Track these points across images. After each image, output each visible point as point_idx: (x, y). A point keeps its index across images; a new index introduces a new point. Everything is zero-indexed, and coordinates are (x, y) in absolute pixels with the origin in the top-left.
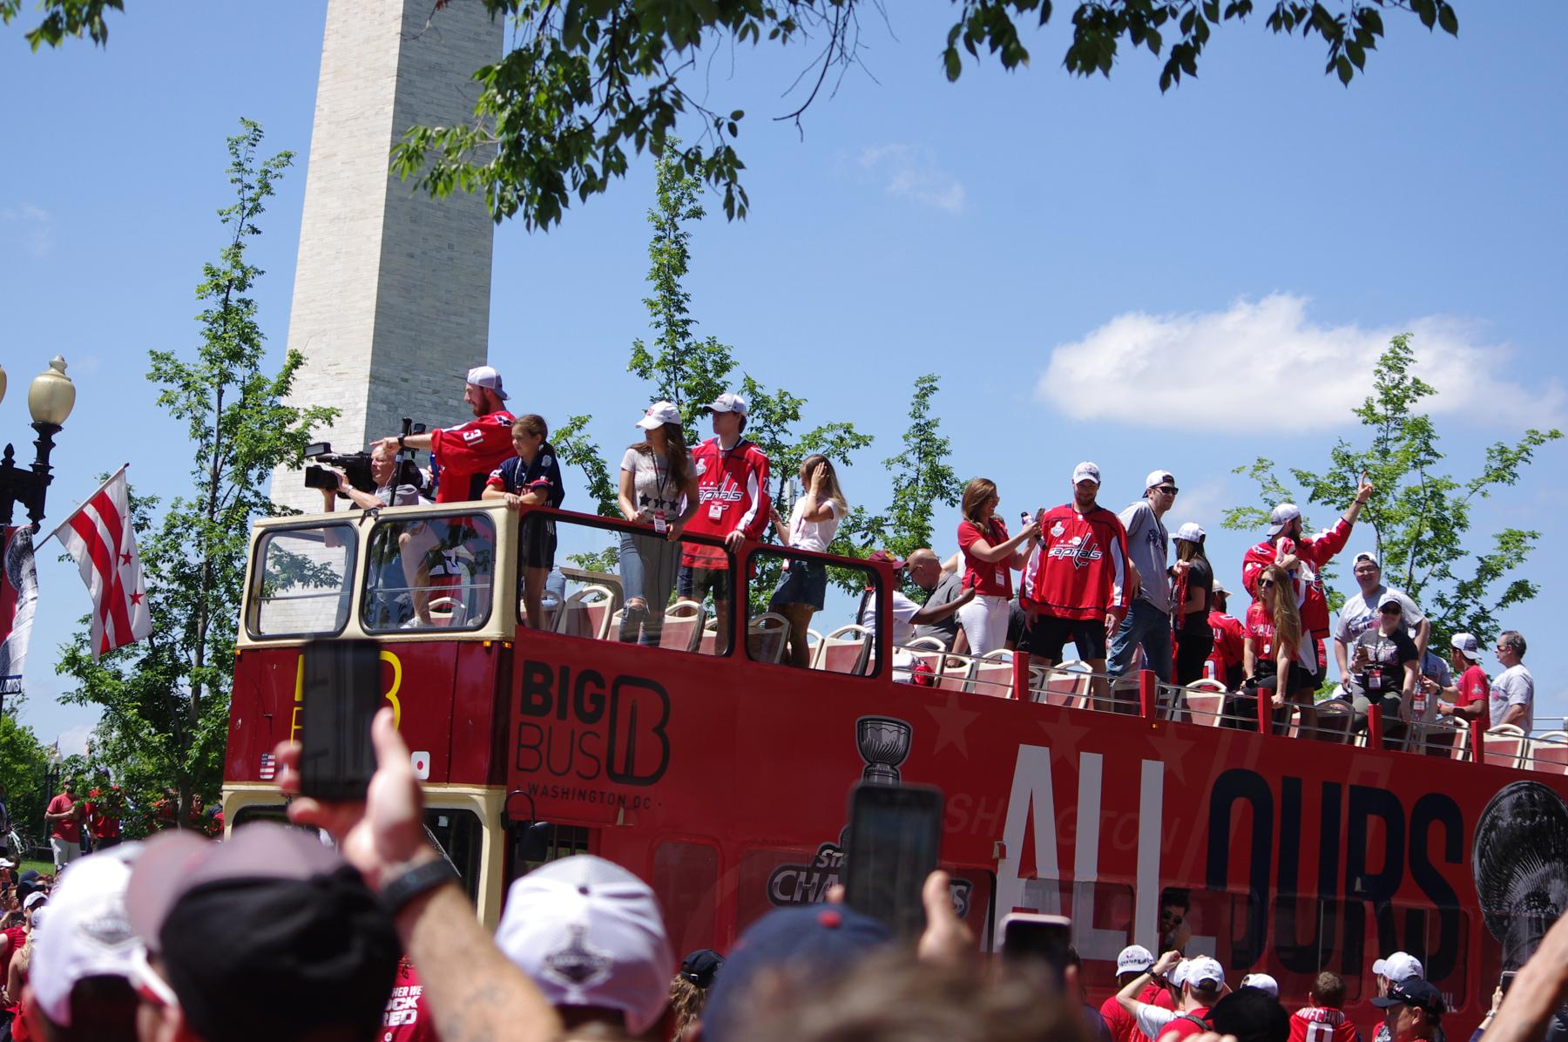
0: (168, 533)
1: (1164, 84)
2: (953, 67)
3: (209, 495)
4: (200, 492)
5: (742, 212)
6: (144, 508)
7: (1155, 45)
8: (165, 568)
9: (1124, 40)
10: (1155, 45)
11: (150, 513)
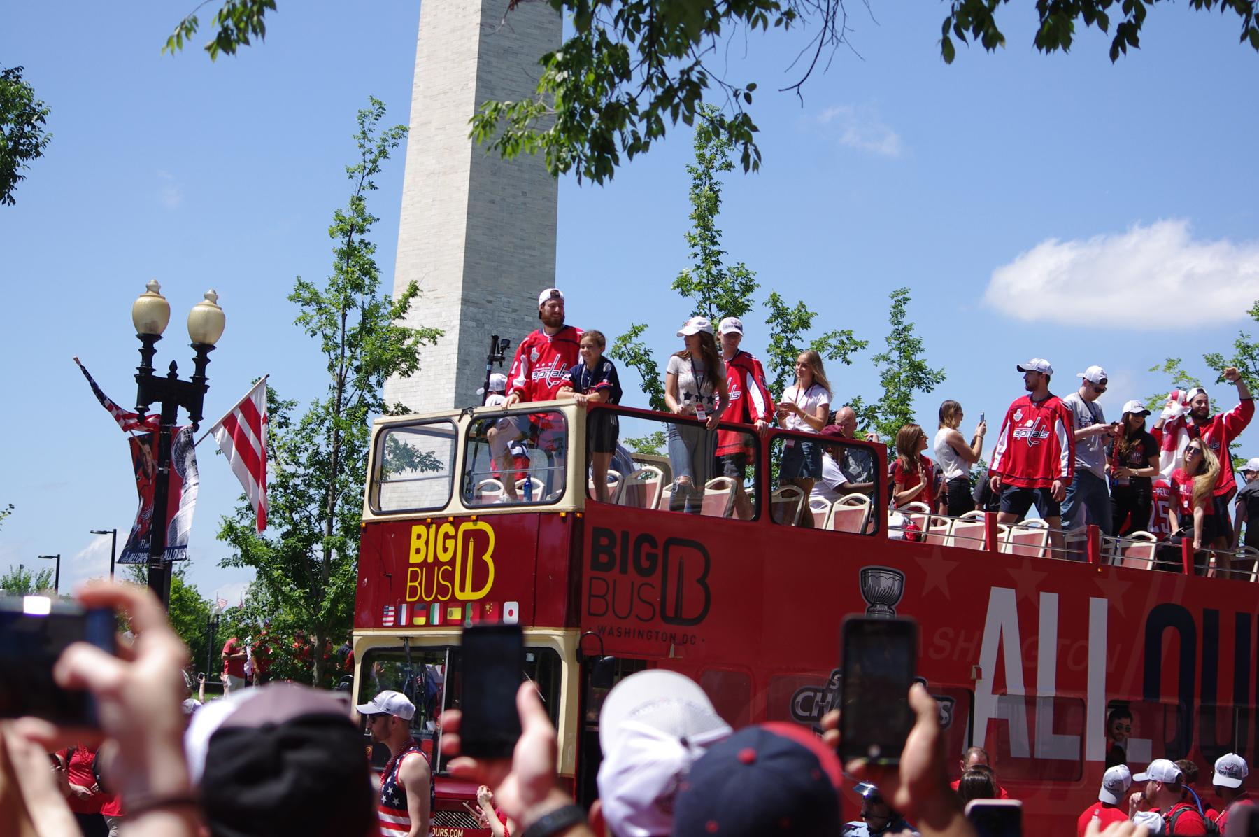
0: (303, 429)
1: (1114, 55)
7: (1104, 25)
8: (303, 457)
9: (1079, 22)
10: (1104, 25)
11: (289, 414)
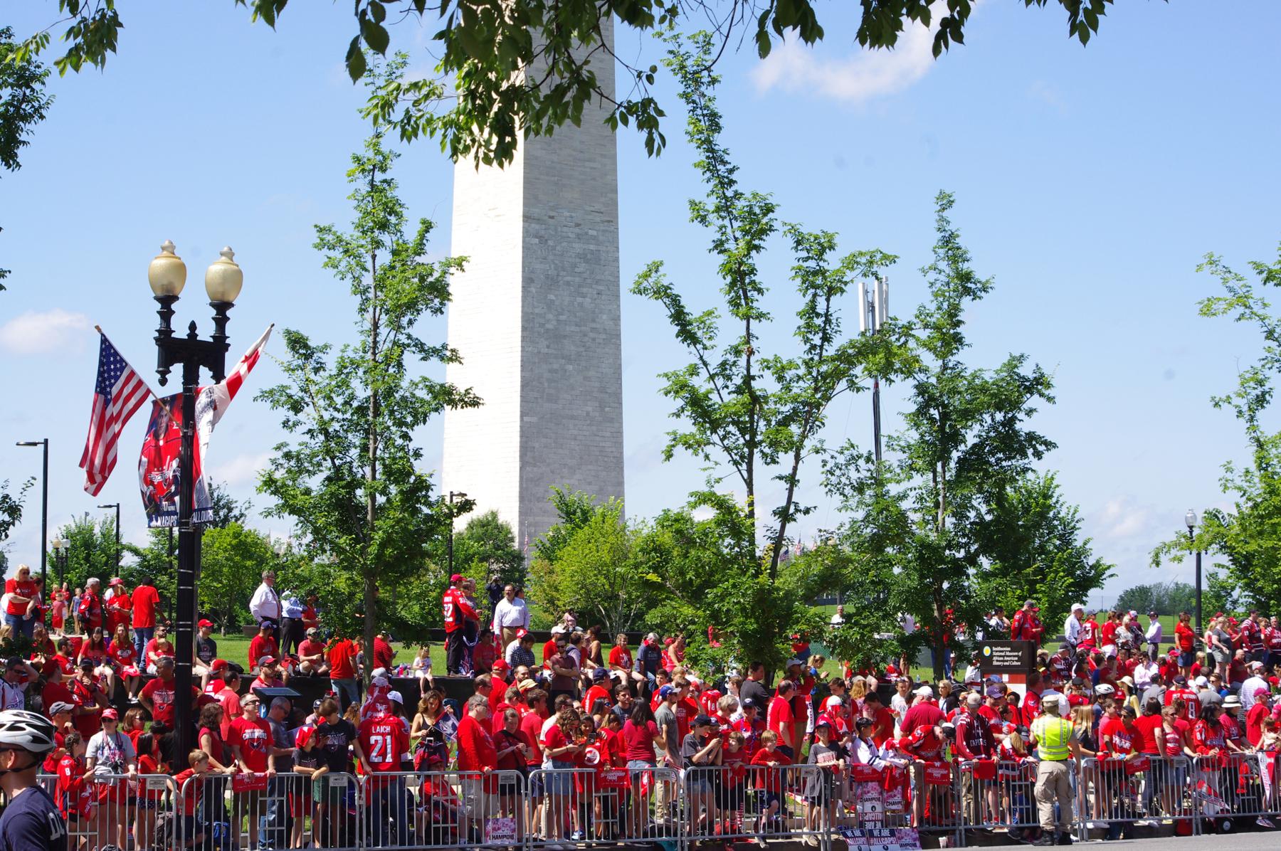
0: (340, 373)
1: (936, 51)
2: (764, 49)
3: (371, 339)
4: (363, 338)
5: (658, 154)
6: (320, 354)
7: (926, 21)
8: (339, 400)
10: (926, 21)
11: (324, 358)
